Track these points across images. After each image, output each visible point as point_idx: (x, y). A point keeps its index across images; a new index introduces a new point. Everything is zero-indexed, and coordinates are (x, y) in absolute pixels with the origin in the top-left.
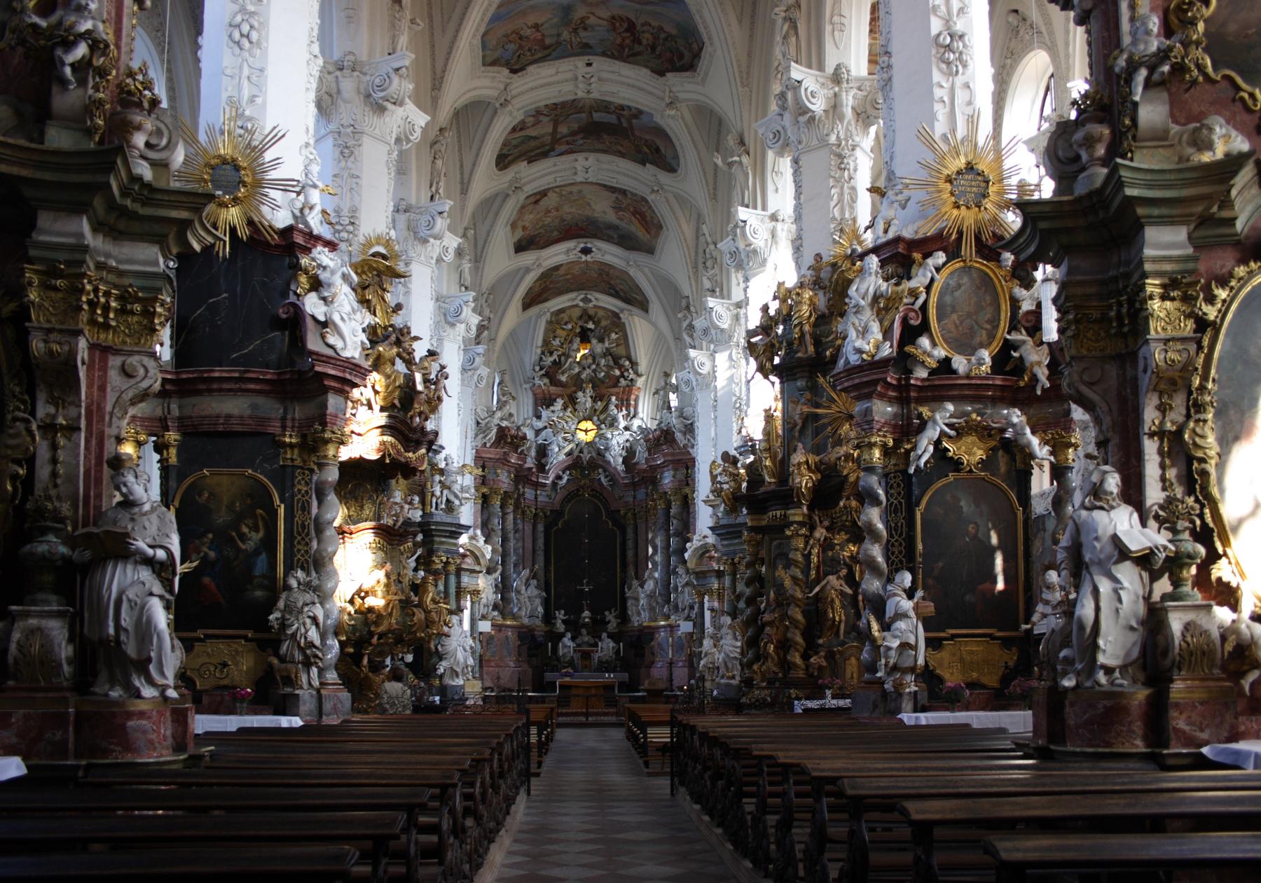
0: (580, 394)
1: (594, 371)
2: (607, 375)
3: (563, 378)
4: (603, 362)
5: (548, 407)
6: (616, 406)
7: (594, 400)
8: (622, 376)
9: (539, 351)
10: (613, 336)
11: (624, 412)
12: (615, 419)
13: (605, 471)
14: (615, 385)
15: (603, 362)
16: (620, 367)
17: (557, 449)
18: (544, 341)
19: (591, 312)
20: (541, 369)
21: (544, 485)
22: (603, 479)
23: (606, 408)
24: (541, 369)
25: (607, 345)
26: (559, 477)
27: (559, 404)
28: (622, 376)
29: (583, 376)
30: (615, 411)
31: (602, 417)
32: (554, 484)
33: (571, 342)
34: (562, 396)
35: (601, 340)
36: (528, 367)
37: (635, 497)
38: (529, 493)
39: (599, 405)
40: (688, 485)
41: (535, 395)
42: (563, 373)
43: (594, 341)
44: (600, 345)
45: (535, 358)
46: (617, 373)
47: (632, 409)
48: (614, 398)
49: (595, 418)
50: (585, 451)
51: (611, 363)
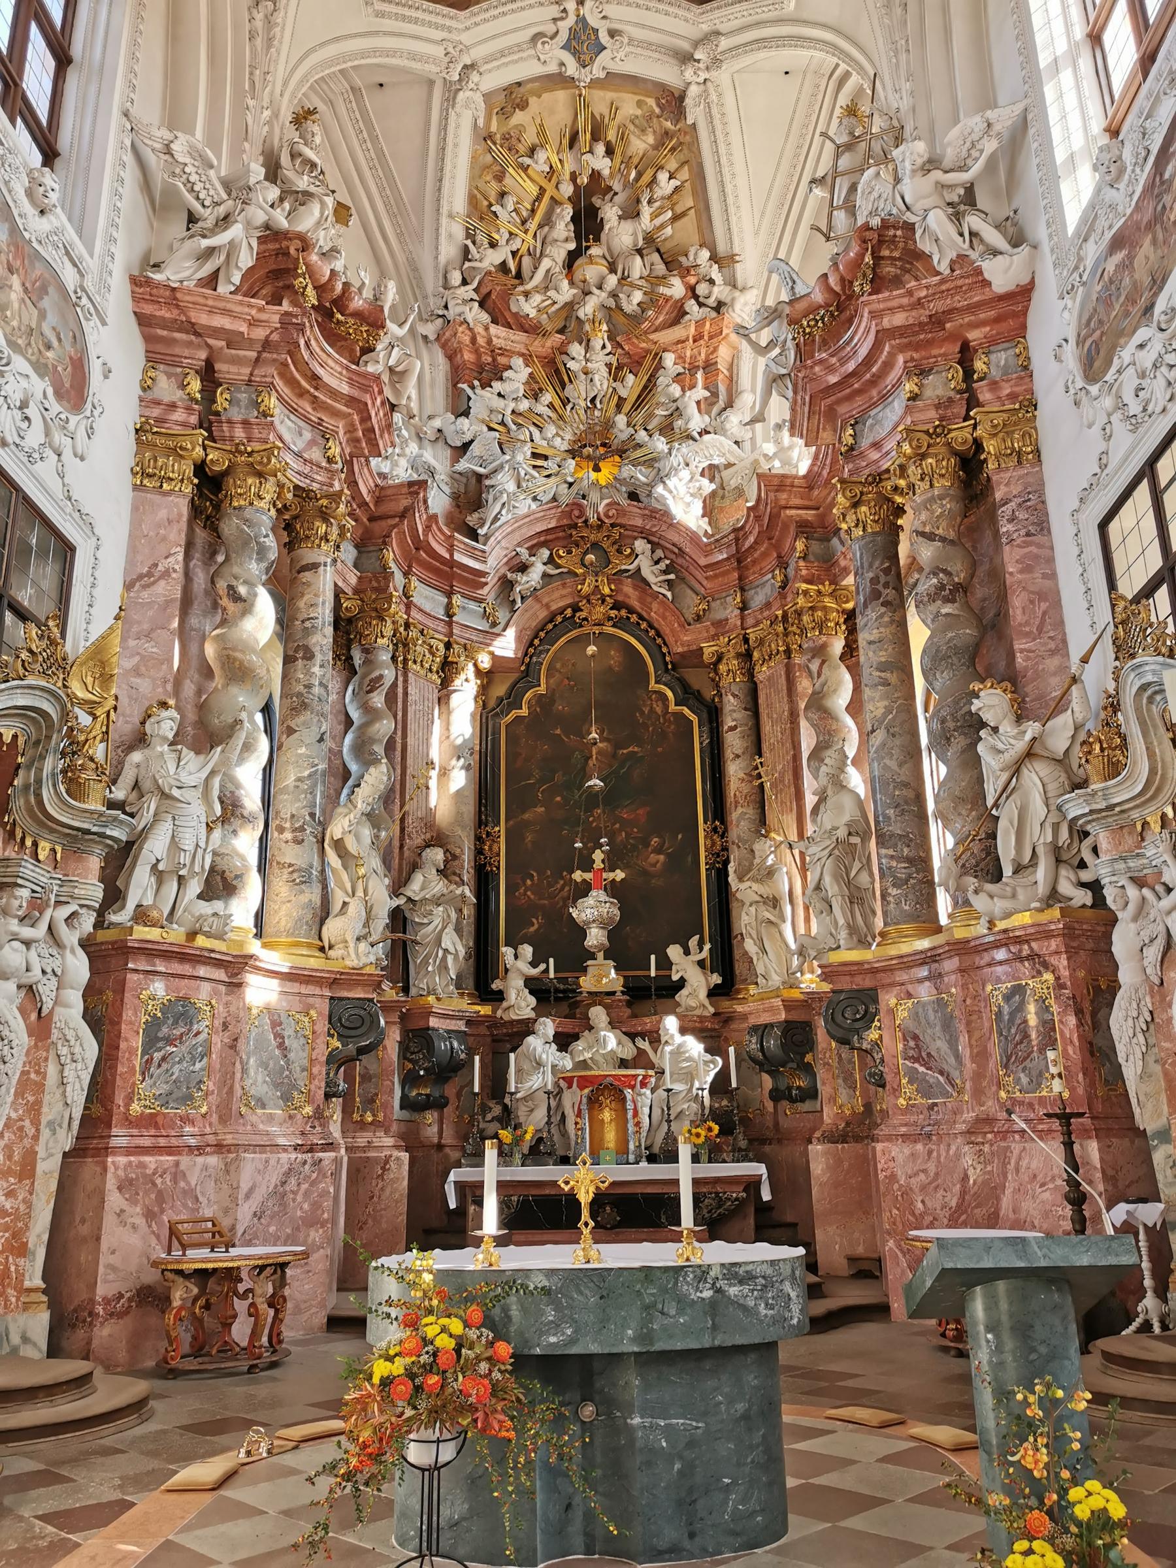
0: (576, 349)
1: (614, 295)
2: (652, 300)
3: (528, 308)
4: (637, 267)
5: (486, 385)
6: (678, 378)
7: (616, 373)
8: (692, 291)
9: (459, 233)
10: (665, 185)
11: (700, 393)
12: (677, 412)
13: (655, 546)
14: (679, 314)
15: (637, 267)
16: (685, 272)
17: (511, 487)
18: (472, 201)
19: (600, 102)
20: (465, 282)
21: (475, 579)
22: (648, 572)
23: (649, 388)
24: (465, 282)
25: (646, 221)
26: (523, 568)
27: (518, 375)
28: (692, 291)
29: (588, 309)
30: (676, 390)
31: (639, 418)
32: (506, 585)
33: (547, 221)
34: (528, 359)
35: (631, 213)
36: (431, 283)
37: (744, 607)
38: (428, 599)
39: (631, 385)
40: (973, 402)
41: (450, 357)
42: (527, 294)
43: (610, 213)
44: (628, 227)
45: (448, 251)
46: (676, 288)
47: (722, 389)
48: (669, 359)
49: (621, 420)
50: (594, 496)
51: (661, 268)
